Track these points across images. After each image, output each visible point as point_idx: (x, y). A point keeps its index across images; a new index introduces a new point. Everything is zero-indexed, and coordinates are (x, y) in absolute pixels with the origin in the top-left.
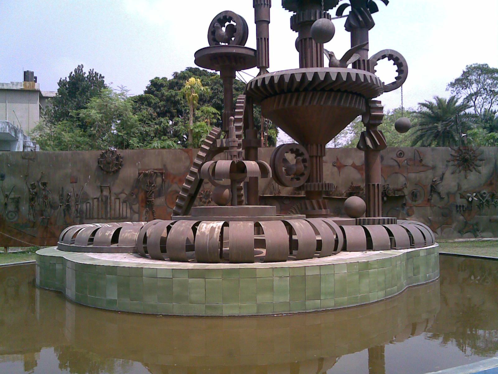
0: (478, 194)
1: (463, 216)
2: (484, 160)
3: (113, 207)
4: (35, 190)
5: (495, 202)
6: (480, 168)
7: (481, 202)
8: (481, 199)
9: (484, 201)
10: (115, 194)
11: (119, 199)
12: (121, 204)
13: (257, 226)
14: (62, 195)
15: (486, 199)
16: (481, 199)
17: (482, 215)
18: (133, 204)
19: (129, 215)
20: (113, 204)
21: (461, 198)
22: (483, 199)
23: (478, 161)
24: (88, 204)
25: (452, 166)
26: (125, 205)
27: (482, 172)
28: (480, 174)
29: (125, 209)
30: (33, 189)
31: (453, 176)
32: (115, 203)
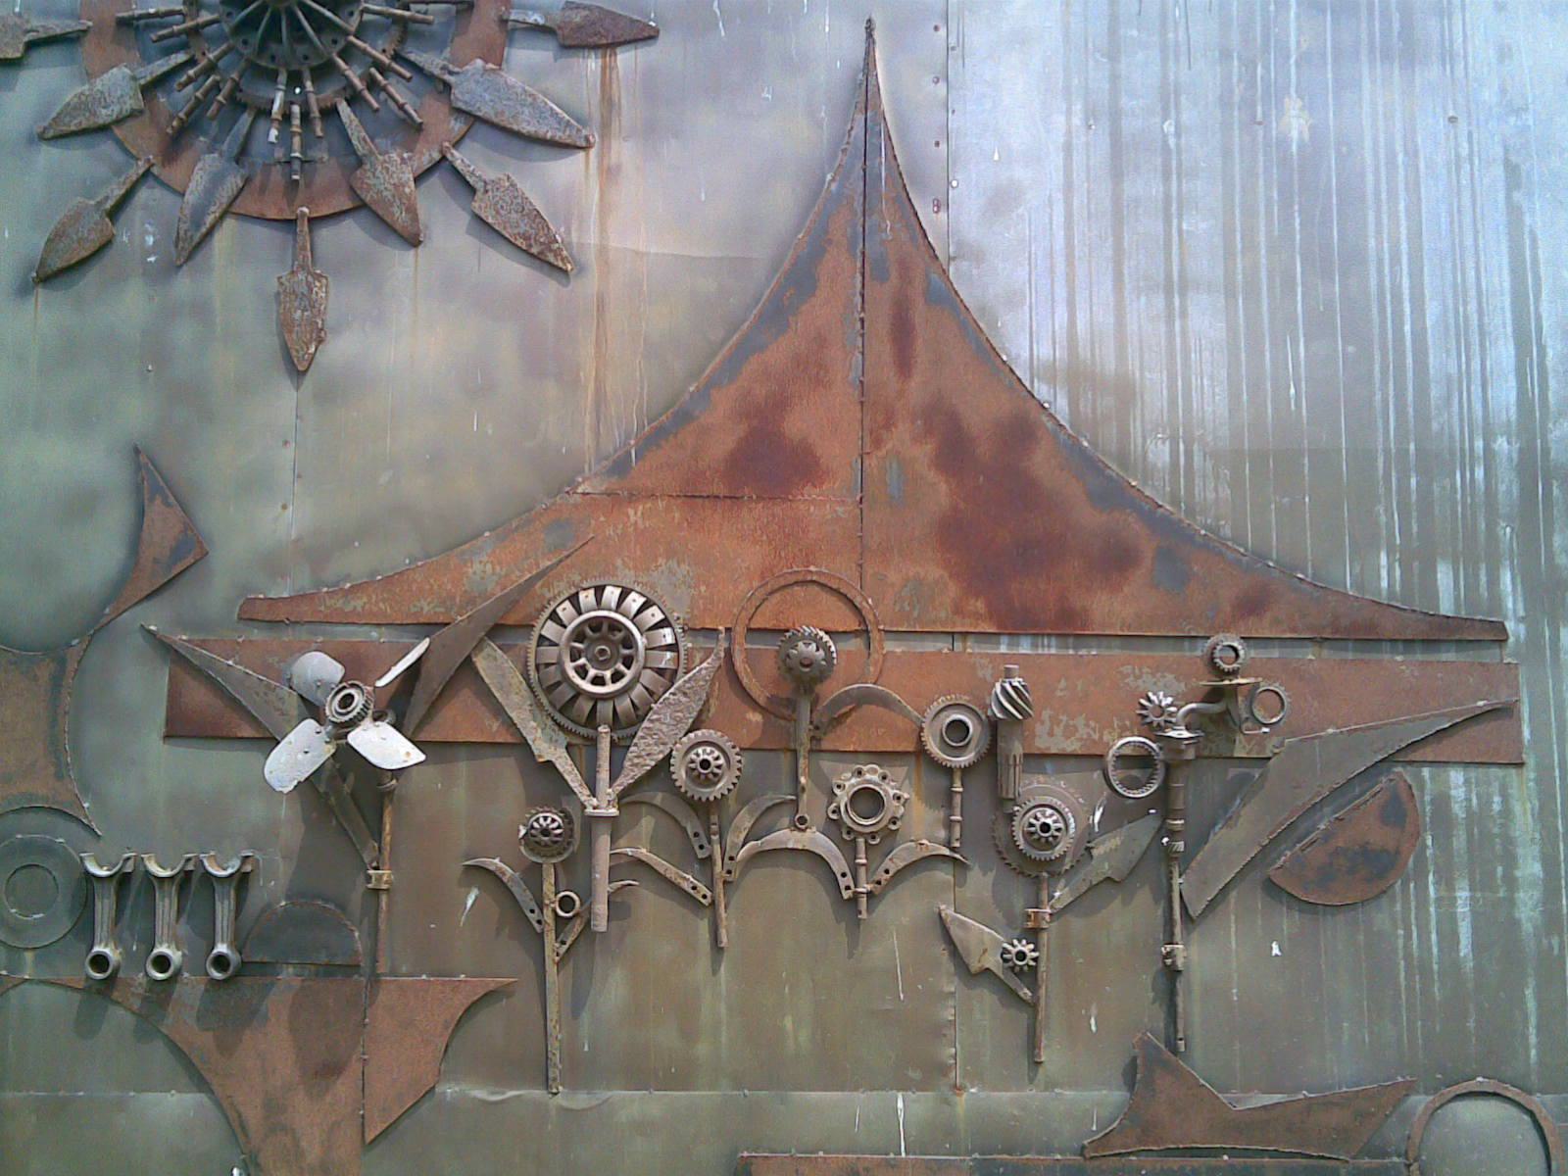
0: (492, 664)
1: (201, 1084)
2: (645, 36)
5: (834, 827)
6: (567, 170)
7: (550, 819)
8: (549, 748)
9: (603, 804)
15: (643, 754)
16: (549, 748)
17: (581, 1072)
21: (181, 728)
22: (583, 749)
23: (527, 58)
25: (49, 154)
27: (584, 237)
28: (550, 287)
31: (48, 312)
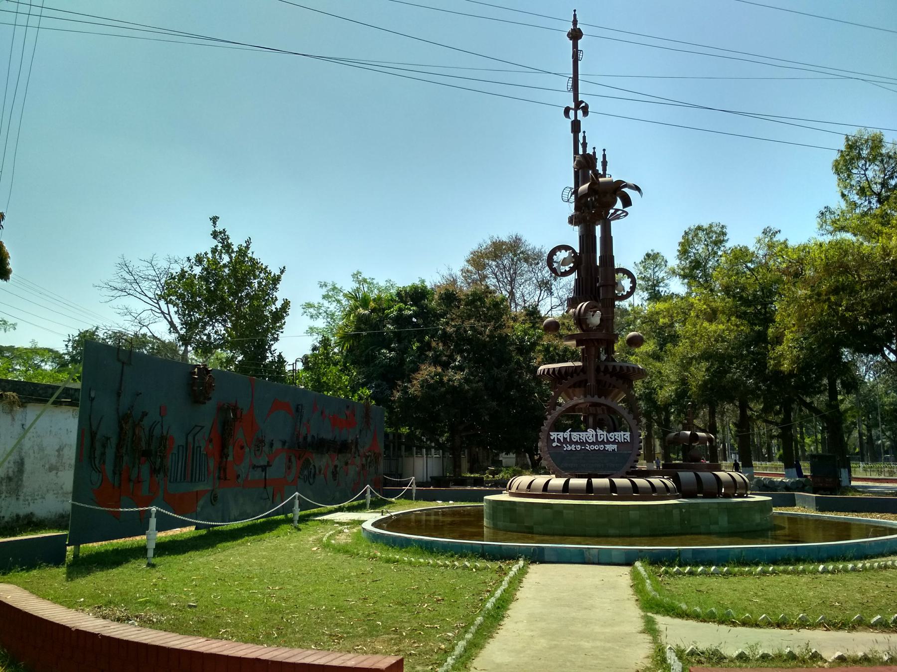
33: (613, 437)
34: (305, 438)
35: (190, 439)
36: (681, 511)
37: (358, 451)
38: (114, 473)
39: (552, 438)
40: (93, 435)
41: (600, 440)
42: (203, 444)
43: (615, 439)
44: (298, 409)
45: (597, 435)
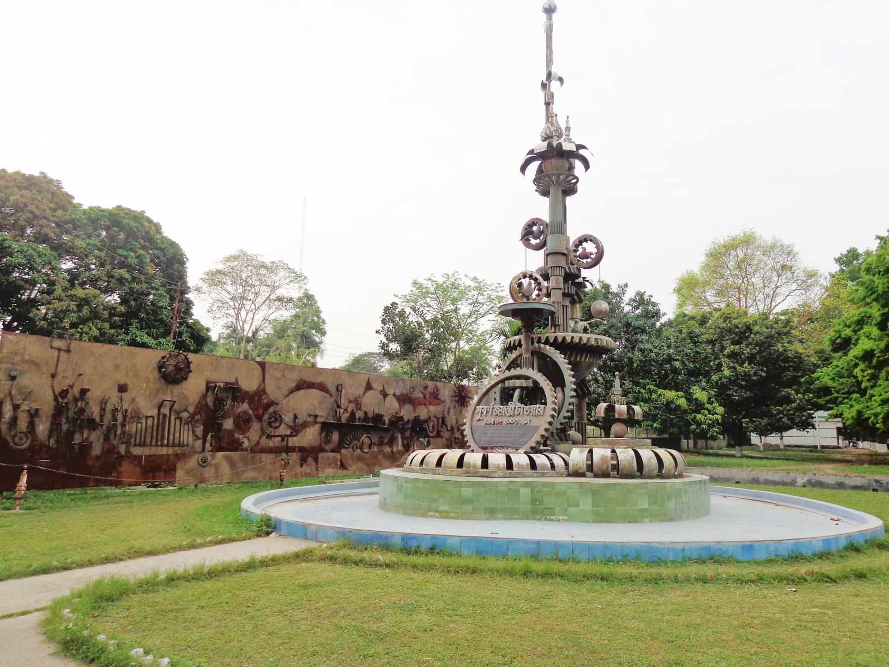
3: (172, 430)
4: (65, 401)
10: (175, 411)
11: (181, 419)
12: (182, 426)
13: (613, 451)
14: (103, 410)
18: (196, 427)
19: (191, 442)
20: (172, 425)
24: (139, 425)
26: (186, 427)
29: (186, 432)
30: (63, 398)
32: (175, 423)
33: (528, 410)
34: (353, 414)
35: (165, 411)
36: (533, 491)
37: (446, 426)
38: (50, 437)
39: (477, 411)
40: (16, 407)
41: (516, 413)
42: (185, 415)
43: (530, 412)
44: (339, 389)
45: (515, 408)
